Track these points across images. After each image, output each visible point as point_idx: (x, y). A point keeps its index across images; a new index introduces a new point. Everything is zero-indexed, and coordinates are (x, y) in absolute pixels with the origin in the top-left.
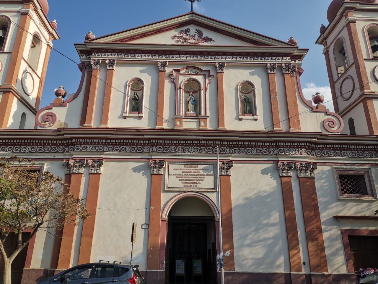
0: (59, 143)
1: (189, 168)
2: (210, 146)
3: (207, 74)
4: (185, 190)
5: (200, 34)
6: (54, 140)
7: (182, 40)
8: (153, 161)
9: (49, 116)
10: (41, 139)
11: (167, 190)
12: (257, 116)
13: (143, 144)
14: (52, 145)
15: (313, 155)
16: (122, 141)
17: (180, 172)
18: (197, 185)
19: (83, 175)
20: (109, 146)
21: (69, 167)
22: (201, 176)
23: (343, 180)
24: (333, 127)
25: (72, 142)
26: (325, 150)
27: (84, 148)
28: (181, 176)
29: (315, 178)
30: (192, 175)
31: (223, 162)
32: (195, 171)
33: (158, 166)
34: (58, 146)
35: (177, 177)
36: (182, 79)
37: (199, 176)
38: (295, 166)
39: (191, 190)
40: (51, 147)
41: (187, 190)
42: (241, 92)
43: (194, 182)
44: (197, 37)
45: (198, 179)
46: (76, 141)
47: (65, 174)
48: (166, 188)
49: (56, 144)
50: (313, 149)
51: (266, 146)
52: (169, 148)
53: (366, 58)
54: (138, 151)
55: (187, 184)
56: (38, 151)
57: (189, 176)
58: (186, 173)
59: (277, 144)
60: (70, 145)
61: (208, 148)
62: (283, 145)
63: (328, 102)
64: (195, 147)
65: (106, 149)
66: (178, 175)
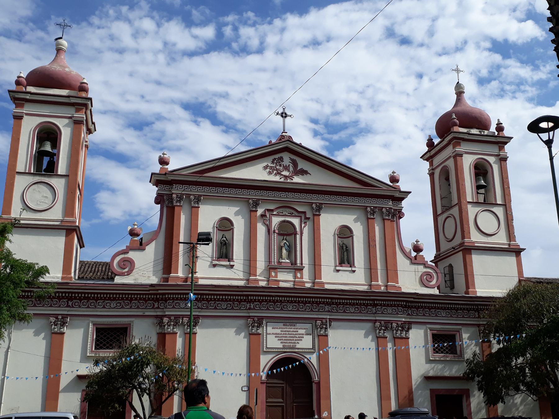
0: (148, 298)
2: (308, 303)
4: (283, 350)
6: (143, 294)
8: (252, 320)
10: (128, 294)
11: (266, 350)
12: (355, 267)
13: (239, 300)
14: (139, 300)
15: (409, 314)
16: (218, 297)
17: (278, 331)
18: (296, 345)
19: (178, 335)
20: (204, 302)
21: (161, 325)
22: (299, 336)
23: (436, 340)
24: (431, 282)
25: (164, 297)
26: (421, 308)
27: (177, 305)
28: (279, 335)
29: (409, 338)
30: (291, 334)
31: (322, 321)
32: (294, 330)
33: (256, 325)
34: (146, 301)
35: (276, 337)
37: (297, 336)
38: (391, 327)
39: (290, 350)
40: (138, 302)
41: (286, 350)
42: (339, 237)
43: (293, 341)
45: (297, 339)
46: (169, 297)
47: (158, 333)
48: (265, 348)
49: (144, 299)
50: (410, 308)
51: (364, 304)
52: (267, 304)
53: (471, 201)
54: (235, 308)
55: (286, 344)
56: (124, 306)
57: (288, 336)
59: (376, 302)
60: (161, 300)
61: (307, 305)
62: (381, 304)
63: (429, 254)
64: (294, 304)
65: (200, 305)
66: (276, 334)
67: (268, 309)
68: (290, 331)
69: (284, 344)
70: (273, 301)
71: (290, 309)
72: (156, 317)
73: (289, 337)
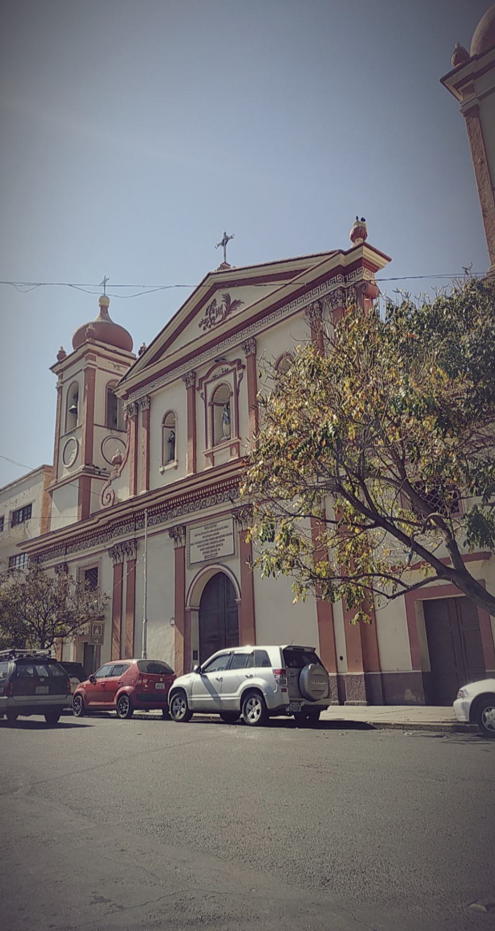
1: (209, 530)
3: (235, 366)
5: (227, 298)
7: (210, 324)
9: (109, 496)
17: (200, 538)
18: (217, 554)
30: (212, 539)
34: (106, 533)
35: (198, 546)
36: (211, 387)
37: (218, 540)
41: (207, 563)
43: (214, 549)
44: (224, 309)
49: (106, 532)
57: (210, 542)
58: (206, 539)
61: (225, 492)
64: (212, 496)
66: (199, 542)
67: (188, 512)
68: (211, 535)
69: (207, 554)
70: (193, 501)
71: (208, 505)
72: (109, 549)
73: (211, 543)
